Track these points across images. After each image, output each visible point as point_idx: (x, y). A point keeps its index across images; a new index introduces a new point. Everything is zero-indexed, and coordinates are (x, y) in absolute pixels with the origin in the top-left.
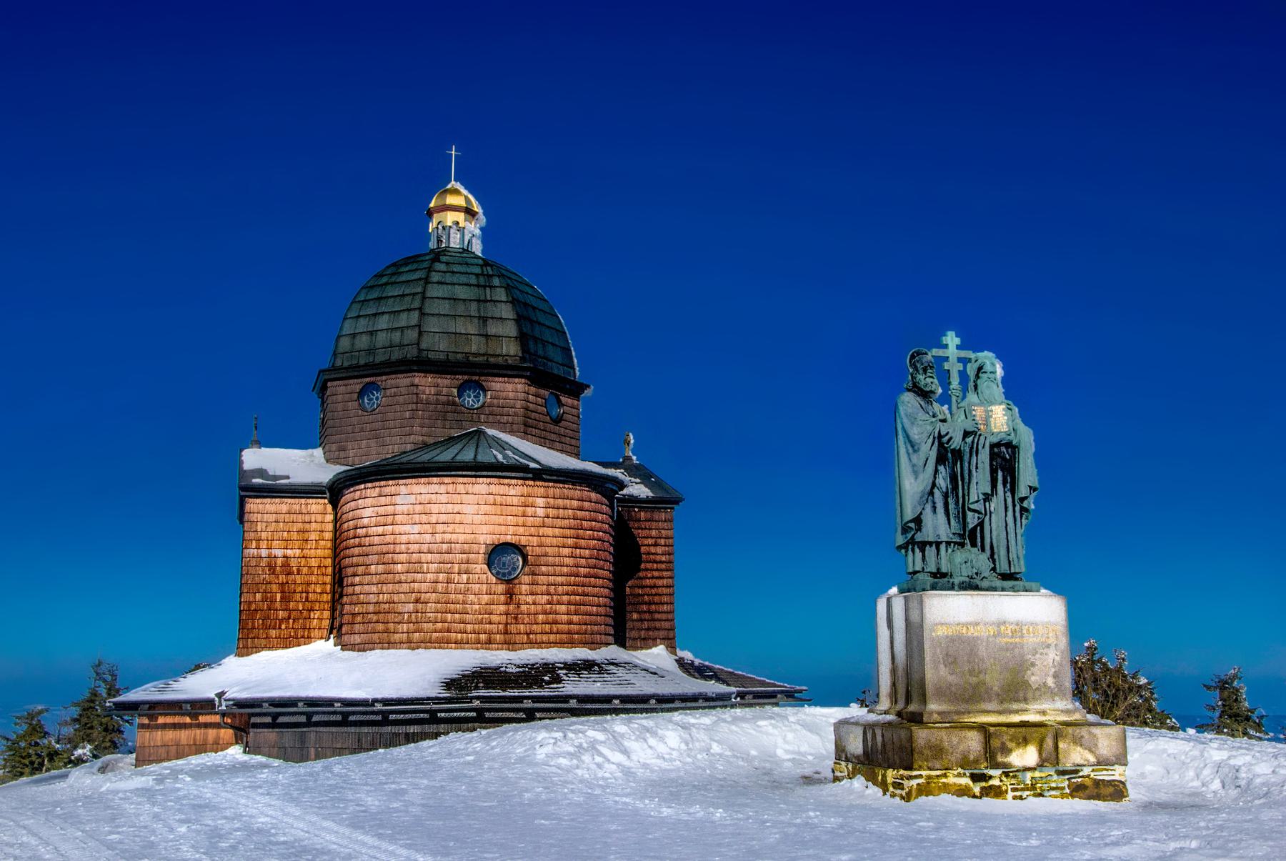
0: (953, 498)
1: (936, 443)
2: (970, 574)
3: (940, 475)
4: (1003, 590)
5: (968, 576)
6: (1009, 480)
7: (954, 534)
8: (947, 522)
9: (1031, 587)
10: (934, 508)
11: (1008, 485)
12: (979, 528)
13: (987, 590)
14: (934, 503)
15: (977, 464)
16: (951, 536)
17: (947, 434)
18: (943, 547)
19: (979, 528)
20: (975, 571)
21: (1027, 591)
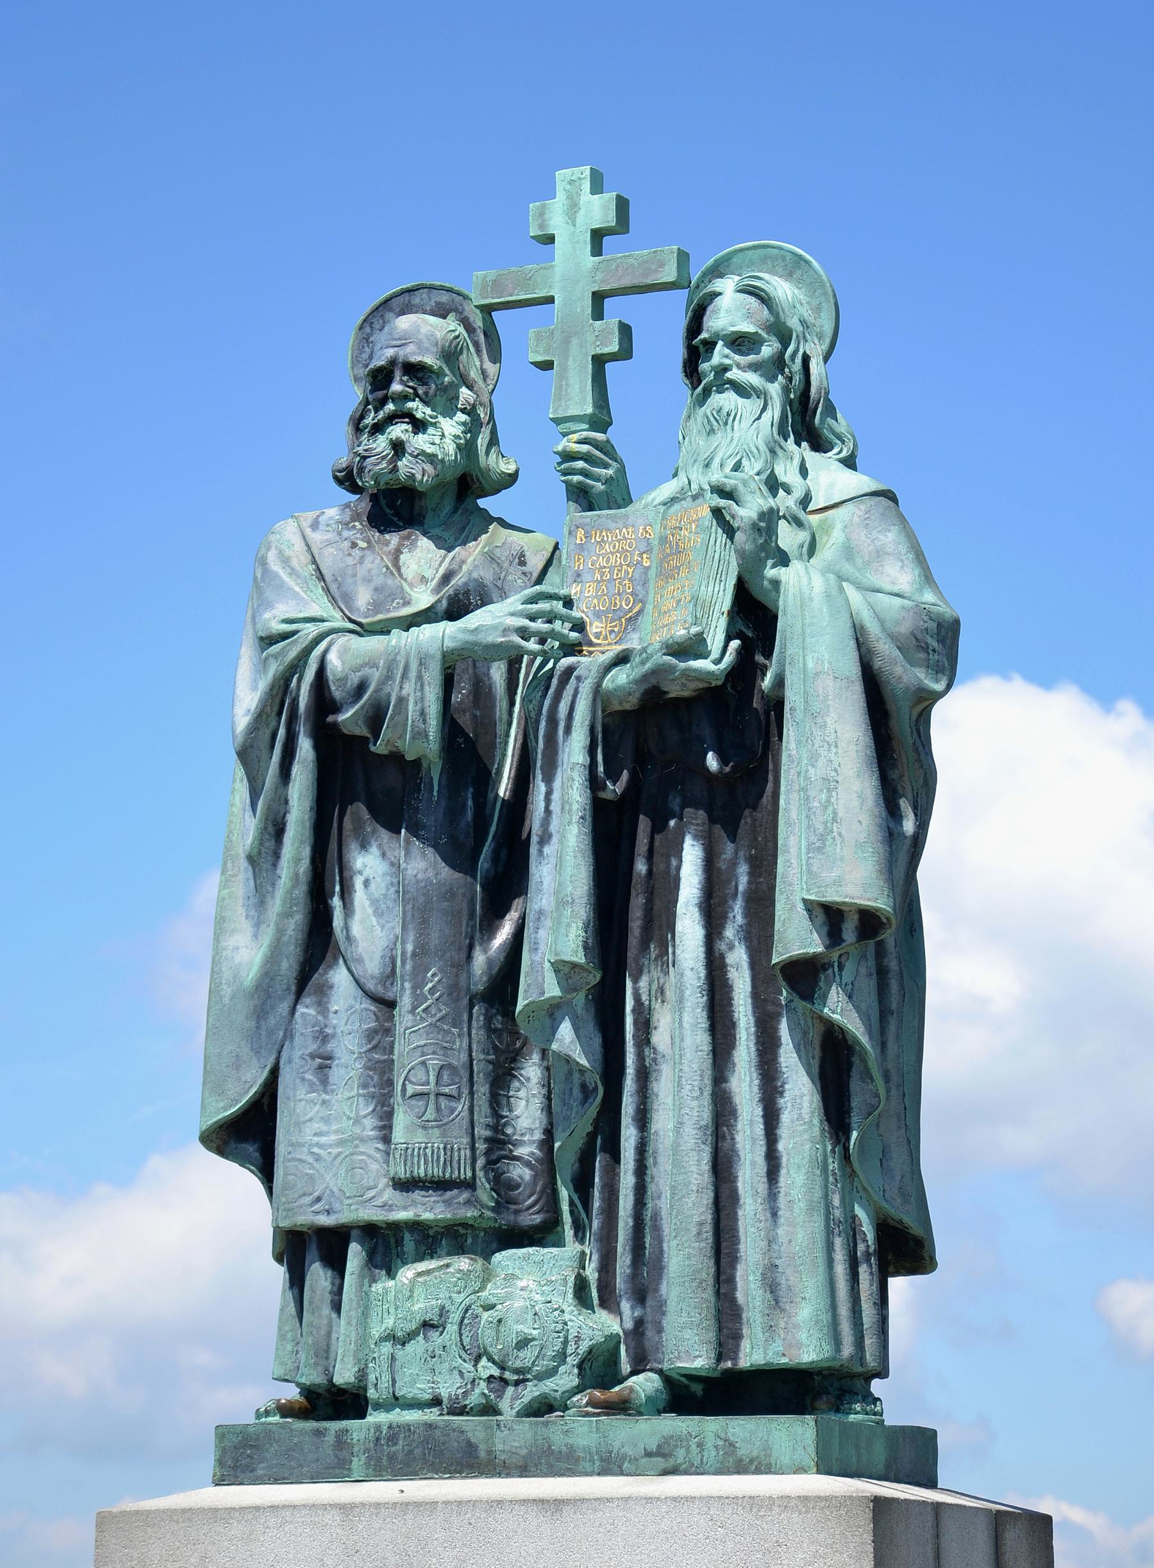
0: (417, 1000)
1: (305, 747)
2: (448, 1388)
3: (360, 896)
4: (610, 1465)
5: (436, 1402)
6: (743, 881)
7: (405, 1185)
8: (370, 1124)
9: (767, 1449)
10: (324, 1063)
11: (737, 913)
12: (599, 1141)
13: (524, 1470)
14: (323, 1037)
15: (548, 811)
16: (389, 1195)
17: (361, 688)
18: (355, 1254)
19: (599, 1141)
20: (487, 1369)
21: (741, 1468)
